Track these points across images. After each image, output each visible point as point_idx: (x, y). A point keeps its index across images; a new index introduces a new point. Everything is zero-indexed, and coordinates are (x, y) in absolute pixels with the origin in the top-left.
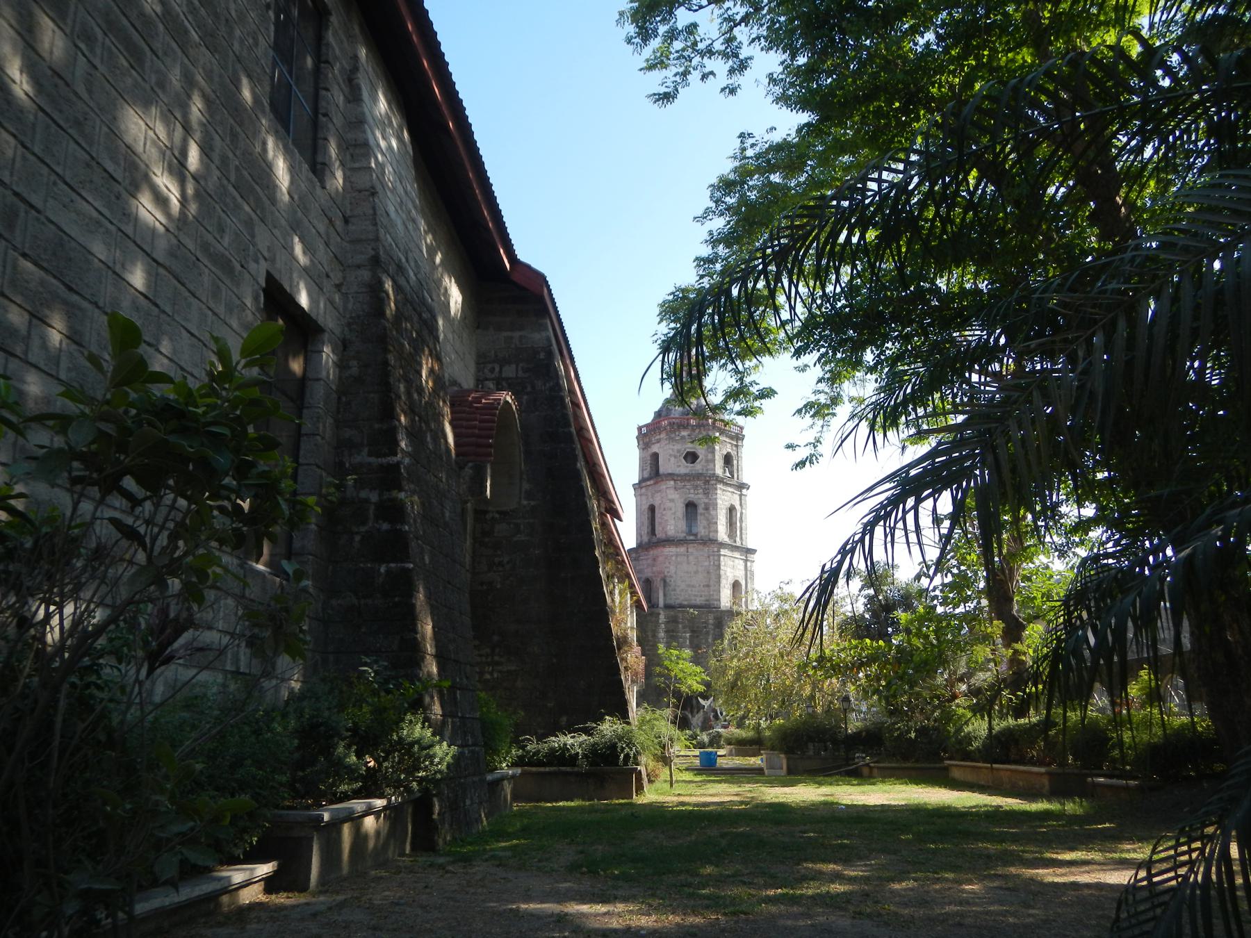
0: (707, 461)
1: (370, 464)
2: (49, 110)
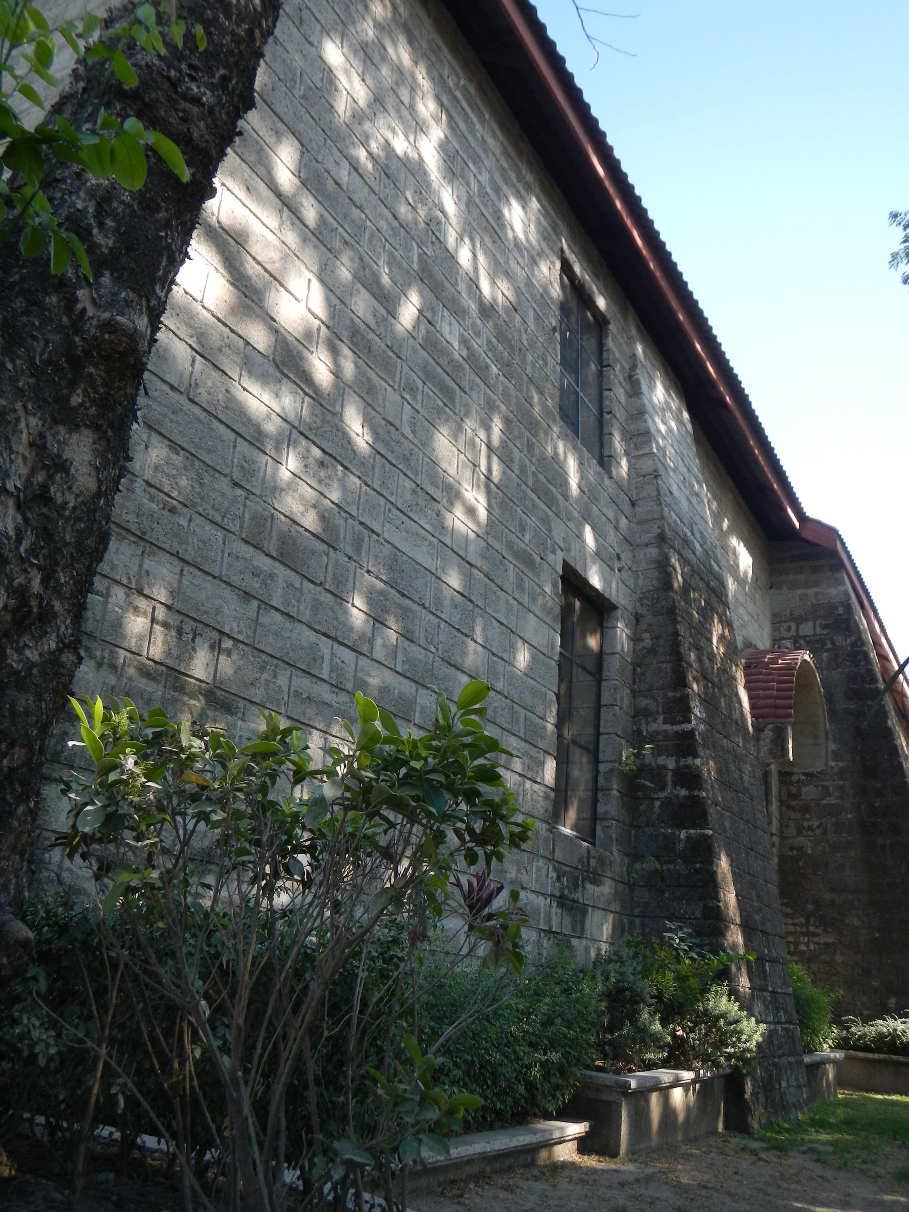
1: (665, 731)
2: (383, 453)
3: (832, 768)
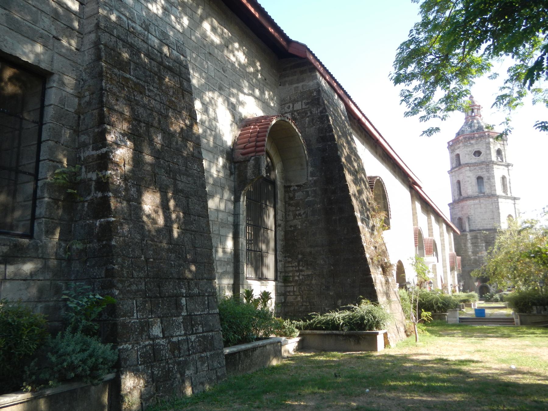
0: (487, 154)
1: (93, 155)
3: (310, 181)
